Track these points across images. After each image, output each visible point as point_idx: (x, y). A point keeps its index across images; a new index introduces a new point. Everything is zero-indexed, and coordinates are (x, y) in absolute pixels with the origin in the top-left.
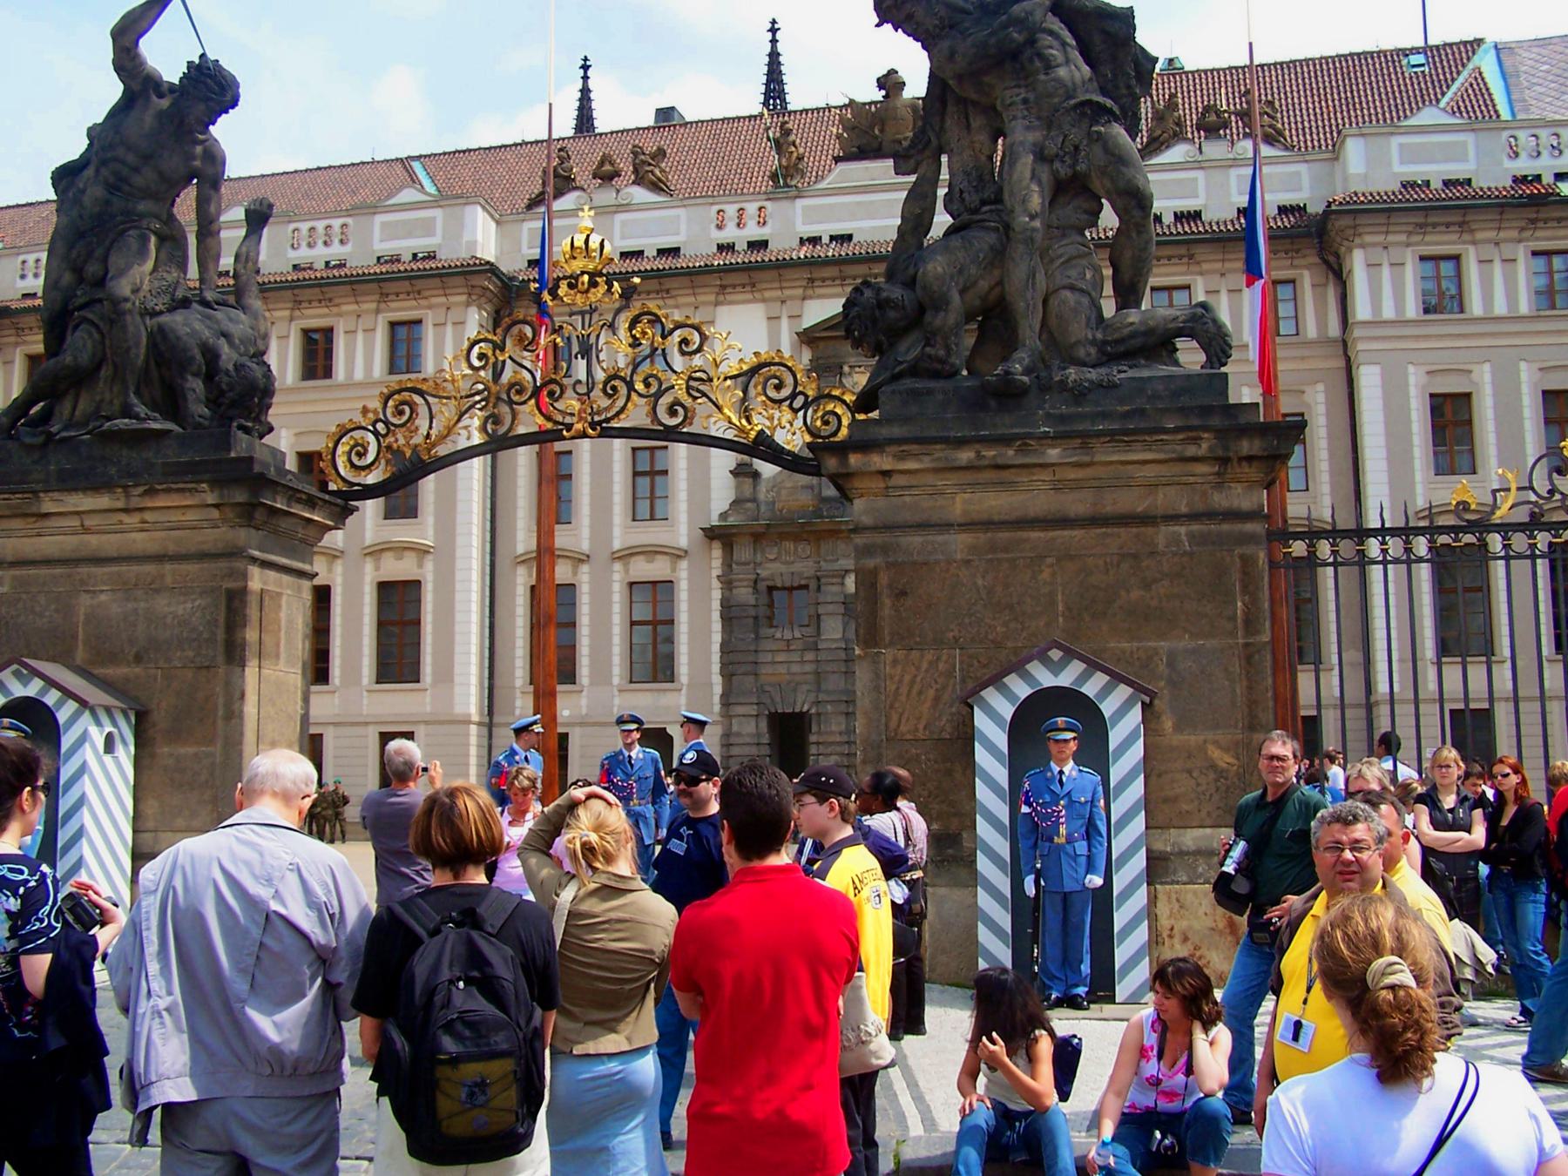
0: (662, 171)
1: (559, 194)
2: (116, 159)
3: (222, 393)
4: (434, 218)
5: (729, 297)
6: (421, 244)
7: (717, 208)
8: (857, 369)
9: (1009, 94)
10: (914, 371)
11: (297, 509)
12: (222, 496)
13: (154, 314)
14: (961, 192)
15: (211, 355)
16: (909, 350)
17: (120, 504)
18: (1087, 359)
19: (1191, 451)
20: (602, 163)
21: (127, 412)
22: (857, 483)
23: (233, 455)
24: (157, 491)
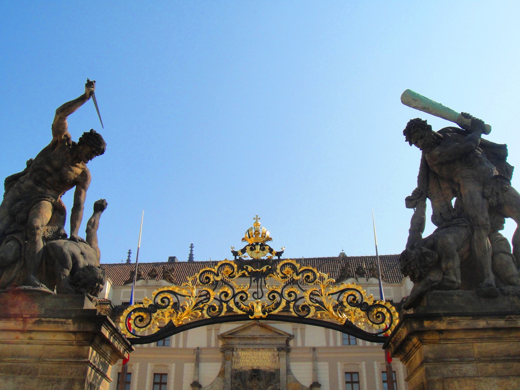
8: (239, 350)
10: (440, 286)
16: (435, 276)
17: (20, 327)
20: (152, 271)
22: (426, 337)
23: (84, 308)
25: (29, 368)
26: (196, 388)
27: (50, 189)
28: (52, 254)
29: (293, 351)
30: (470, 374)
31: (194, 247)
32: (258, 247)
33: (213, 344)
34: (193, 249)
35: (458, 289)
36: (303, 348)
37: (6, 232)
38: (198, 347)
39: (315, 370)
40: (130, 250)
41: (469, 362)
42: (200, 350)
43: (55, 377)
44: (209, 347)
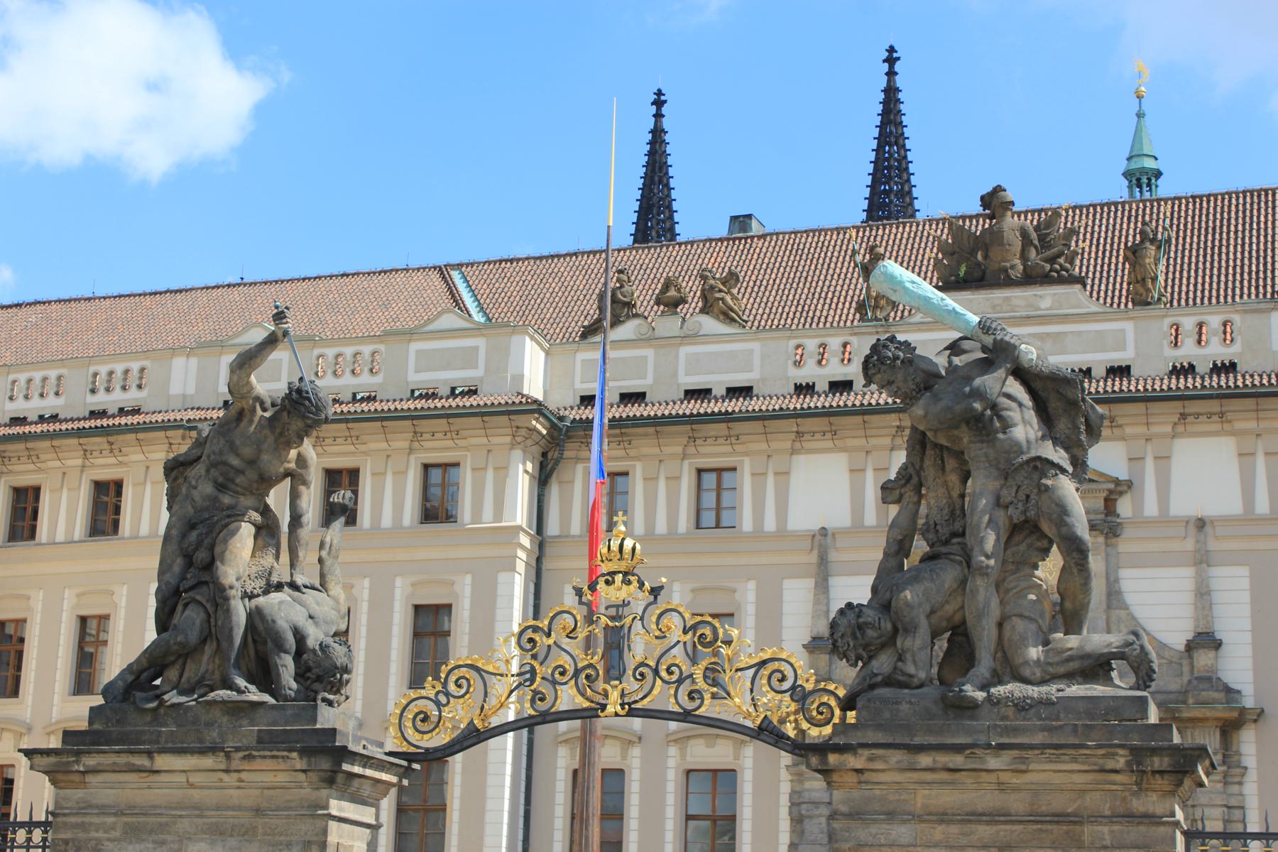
0: (734, 298)
1: (616, 322)
2: (225, 463)
3: (309, 669)
4: (476, 348)
5: (807, 445)
6: (460, 376)
7: (793, 343)
9: (975, 451)
10: (889, 682)
11: (369, 772)
12: (309, 765)
13: (251, 596)
14: (936, 525)
15: (300, 637)
16: (883, 664)
17: (223, 767)
18: (1033, 678)
19: (1110, 764)
20: (666, 287)
21: (230, 686)
22: (835, 777)
23: (318, 726)
24: (254, 757)
25: (243, 825)
26: (822, 656)
27: (243, 494)
28: (260, 627)
29: (1127, 533)
30: (904, 841)
31: (898, 59)
32: (619, 578)
33: (870, 518)
34: (897, 67)
35: (921, 686)
36: (1165, 519)
37: (181, 589)
38: (823, 528)
39: (1202, 595)
40: (659, 91)
41: (904, 822)
42: (829, 538)
43: (282, 838)
44: (858, 527)
